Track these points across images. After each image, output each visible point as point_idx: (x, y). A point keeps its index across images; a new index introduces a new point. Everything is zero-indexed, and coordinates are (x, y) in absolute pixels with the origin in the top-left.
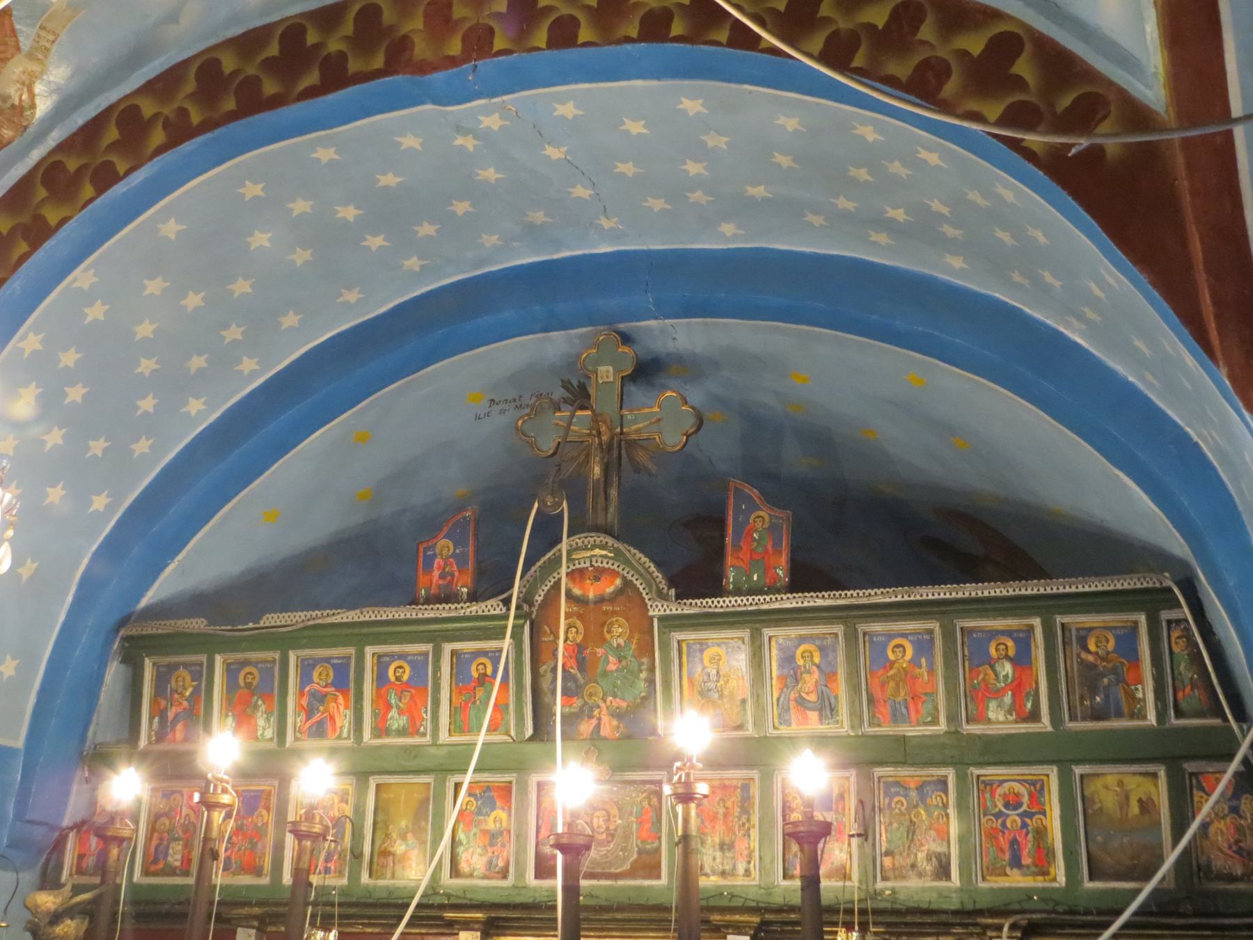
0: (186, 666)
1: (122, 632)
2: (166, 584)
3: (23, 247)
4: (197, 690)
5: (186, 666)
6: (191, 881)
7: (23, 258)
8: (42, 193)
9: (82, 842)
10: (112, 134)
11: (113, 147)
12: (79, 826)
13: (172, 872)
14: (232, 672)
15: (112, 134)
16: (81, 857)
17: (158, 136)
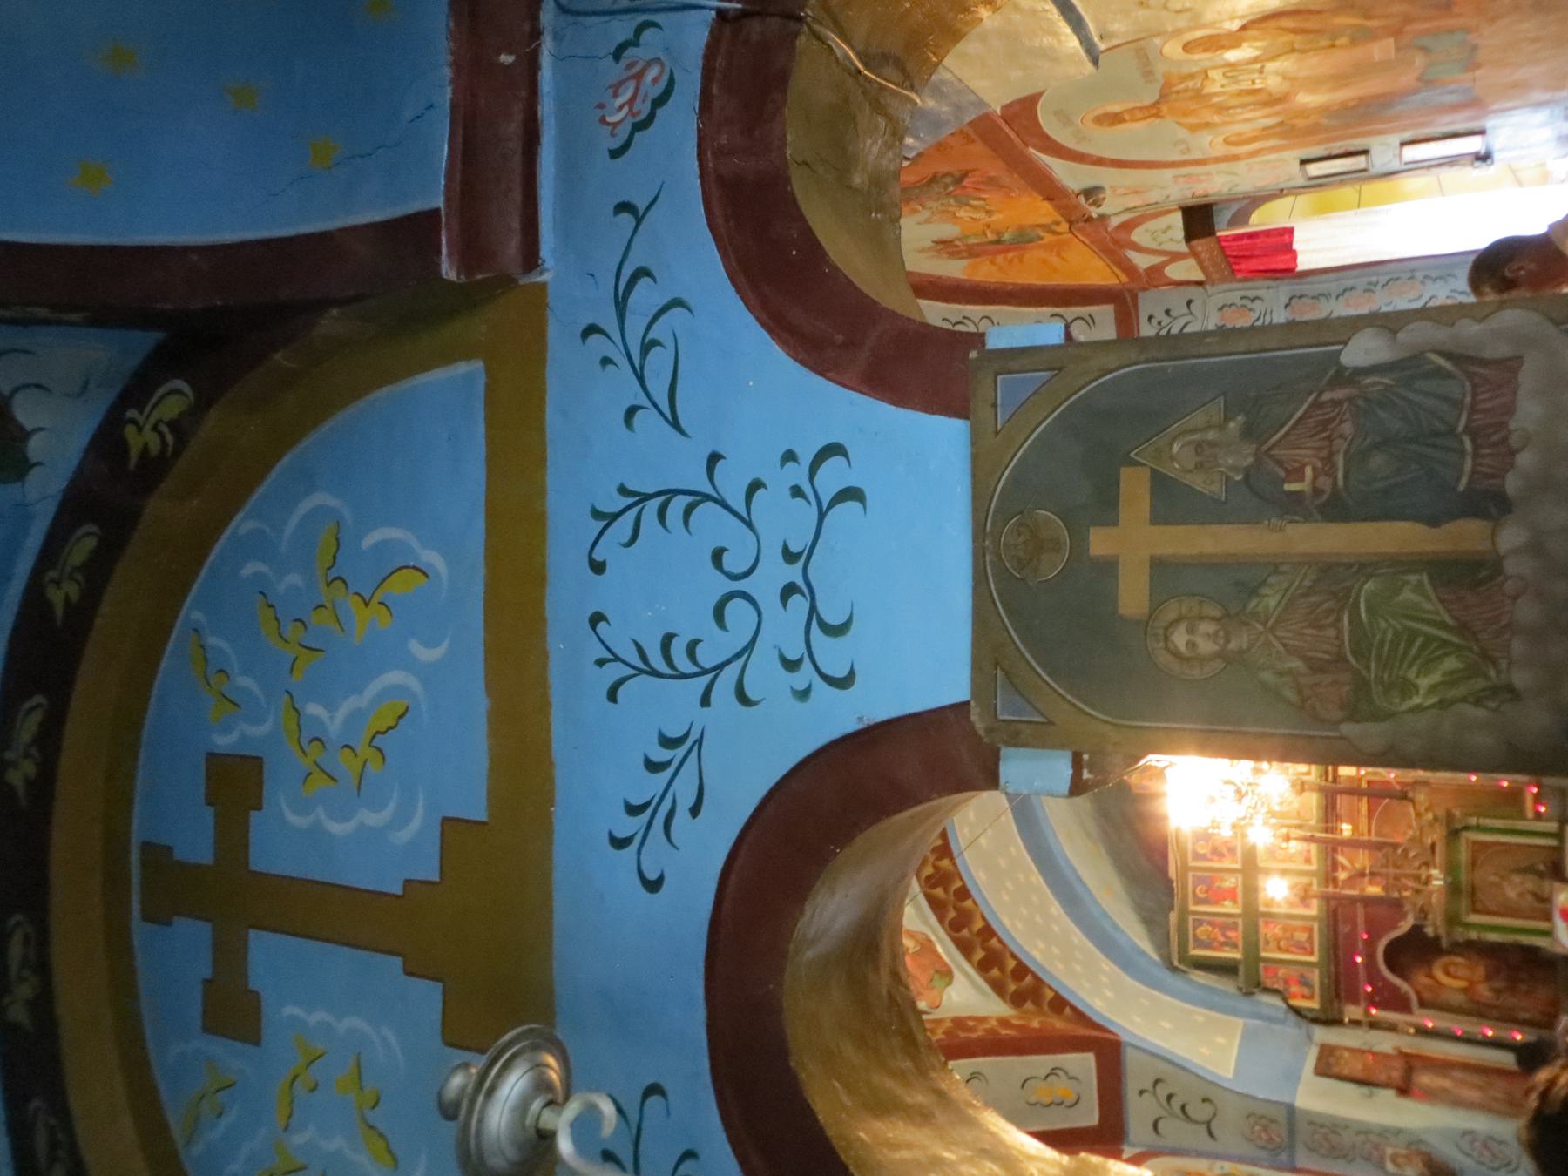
0: (1195, 929)
1: (1176, 963)
2: (1146, 946)
3: (994, 941)
4: (1210, 923)
5: (1195, 929)
6: (1316, 926)
7: (1000, 941)
8: (965, 932)
9: (1294, 996)
10: (939, 892)
11: (946, 890)
12: (1285, 1000)
13: (1310, 939)
14: (1199, 902)
15: (939, 892)
16: (1304, 997)
17: (945, 863)
